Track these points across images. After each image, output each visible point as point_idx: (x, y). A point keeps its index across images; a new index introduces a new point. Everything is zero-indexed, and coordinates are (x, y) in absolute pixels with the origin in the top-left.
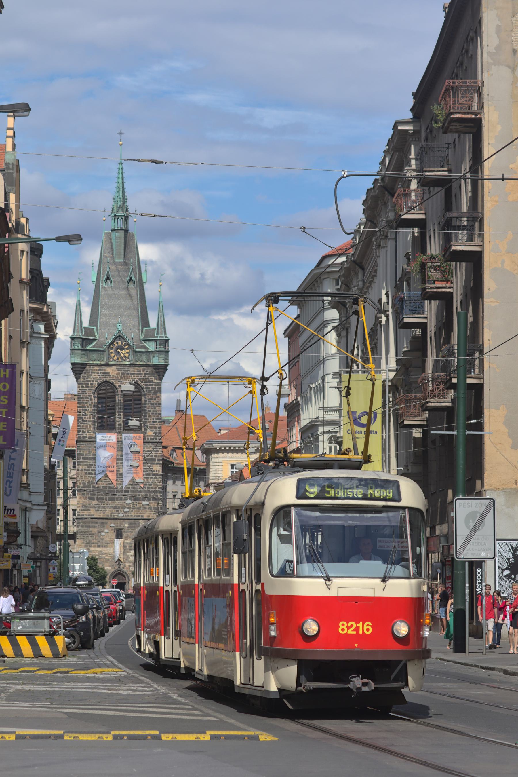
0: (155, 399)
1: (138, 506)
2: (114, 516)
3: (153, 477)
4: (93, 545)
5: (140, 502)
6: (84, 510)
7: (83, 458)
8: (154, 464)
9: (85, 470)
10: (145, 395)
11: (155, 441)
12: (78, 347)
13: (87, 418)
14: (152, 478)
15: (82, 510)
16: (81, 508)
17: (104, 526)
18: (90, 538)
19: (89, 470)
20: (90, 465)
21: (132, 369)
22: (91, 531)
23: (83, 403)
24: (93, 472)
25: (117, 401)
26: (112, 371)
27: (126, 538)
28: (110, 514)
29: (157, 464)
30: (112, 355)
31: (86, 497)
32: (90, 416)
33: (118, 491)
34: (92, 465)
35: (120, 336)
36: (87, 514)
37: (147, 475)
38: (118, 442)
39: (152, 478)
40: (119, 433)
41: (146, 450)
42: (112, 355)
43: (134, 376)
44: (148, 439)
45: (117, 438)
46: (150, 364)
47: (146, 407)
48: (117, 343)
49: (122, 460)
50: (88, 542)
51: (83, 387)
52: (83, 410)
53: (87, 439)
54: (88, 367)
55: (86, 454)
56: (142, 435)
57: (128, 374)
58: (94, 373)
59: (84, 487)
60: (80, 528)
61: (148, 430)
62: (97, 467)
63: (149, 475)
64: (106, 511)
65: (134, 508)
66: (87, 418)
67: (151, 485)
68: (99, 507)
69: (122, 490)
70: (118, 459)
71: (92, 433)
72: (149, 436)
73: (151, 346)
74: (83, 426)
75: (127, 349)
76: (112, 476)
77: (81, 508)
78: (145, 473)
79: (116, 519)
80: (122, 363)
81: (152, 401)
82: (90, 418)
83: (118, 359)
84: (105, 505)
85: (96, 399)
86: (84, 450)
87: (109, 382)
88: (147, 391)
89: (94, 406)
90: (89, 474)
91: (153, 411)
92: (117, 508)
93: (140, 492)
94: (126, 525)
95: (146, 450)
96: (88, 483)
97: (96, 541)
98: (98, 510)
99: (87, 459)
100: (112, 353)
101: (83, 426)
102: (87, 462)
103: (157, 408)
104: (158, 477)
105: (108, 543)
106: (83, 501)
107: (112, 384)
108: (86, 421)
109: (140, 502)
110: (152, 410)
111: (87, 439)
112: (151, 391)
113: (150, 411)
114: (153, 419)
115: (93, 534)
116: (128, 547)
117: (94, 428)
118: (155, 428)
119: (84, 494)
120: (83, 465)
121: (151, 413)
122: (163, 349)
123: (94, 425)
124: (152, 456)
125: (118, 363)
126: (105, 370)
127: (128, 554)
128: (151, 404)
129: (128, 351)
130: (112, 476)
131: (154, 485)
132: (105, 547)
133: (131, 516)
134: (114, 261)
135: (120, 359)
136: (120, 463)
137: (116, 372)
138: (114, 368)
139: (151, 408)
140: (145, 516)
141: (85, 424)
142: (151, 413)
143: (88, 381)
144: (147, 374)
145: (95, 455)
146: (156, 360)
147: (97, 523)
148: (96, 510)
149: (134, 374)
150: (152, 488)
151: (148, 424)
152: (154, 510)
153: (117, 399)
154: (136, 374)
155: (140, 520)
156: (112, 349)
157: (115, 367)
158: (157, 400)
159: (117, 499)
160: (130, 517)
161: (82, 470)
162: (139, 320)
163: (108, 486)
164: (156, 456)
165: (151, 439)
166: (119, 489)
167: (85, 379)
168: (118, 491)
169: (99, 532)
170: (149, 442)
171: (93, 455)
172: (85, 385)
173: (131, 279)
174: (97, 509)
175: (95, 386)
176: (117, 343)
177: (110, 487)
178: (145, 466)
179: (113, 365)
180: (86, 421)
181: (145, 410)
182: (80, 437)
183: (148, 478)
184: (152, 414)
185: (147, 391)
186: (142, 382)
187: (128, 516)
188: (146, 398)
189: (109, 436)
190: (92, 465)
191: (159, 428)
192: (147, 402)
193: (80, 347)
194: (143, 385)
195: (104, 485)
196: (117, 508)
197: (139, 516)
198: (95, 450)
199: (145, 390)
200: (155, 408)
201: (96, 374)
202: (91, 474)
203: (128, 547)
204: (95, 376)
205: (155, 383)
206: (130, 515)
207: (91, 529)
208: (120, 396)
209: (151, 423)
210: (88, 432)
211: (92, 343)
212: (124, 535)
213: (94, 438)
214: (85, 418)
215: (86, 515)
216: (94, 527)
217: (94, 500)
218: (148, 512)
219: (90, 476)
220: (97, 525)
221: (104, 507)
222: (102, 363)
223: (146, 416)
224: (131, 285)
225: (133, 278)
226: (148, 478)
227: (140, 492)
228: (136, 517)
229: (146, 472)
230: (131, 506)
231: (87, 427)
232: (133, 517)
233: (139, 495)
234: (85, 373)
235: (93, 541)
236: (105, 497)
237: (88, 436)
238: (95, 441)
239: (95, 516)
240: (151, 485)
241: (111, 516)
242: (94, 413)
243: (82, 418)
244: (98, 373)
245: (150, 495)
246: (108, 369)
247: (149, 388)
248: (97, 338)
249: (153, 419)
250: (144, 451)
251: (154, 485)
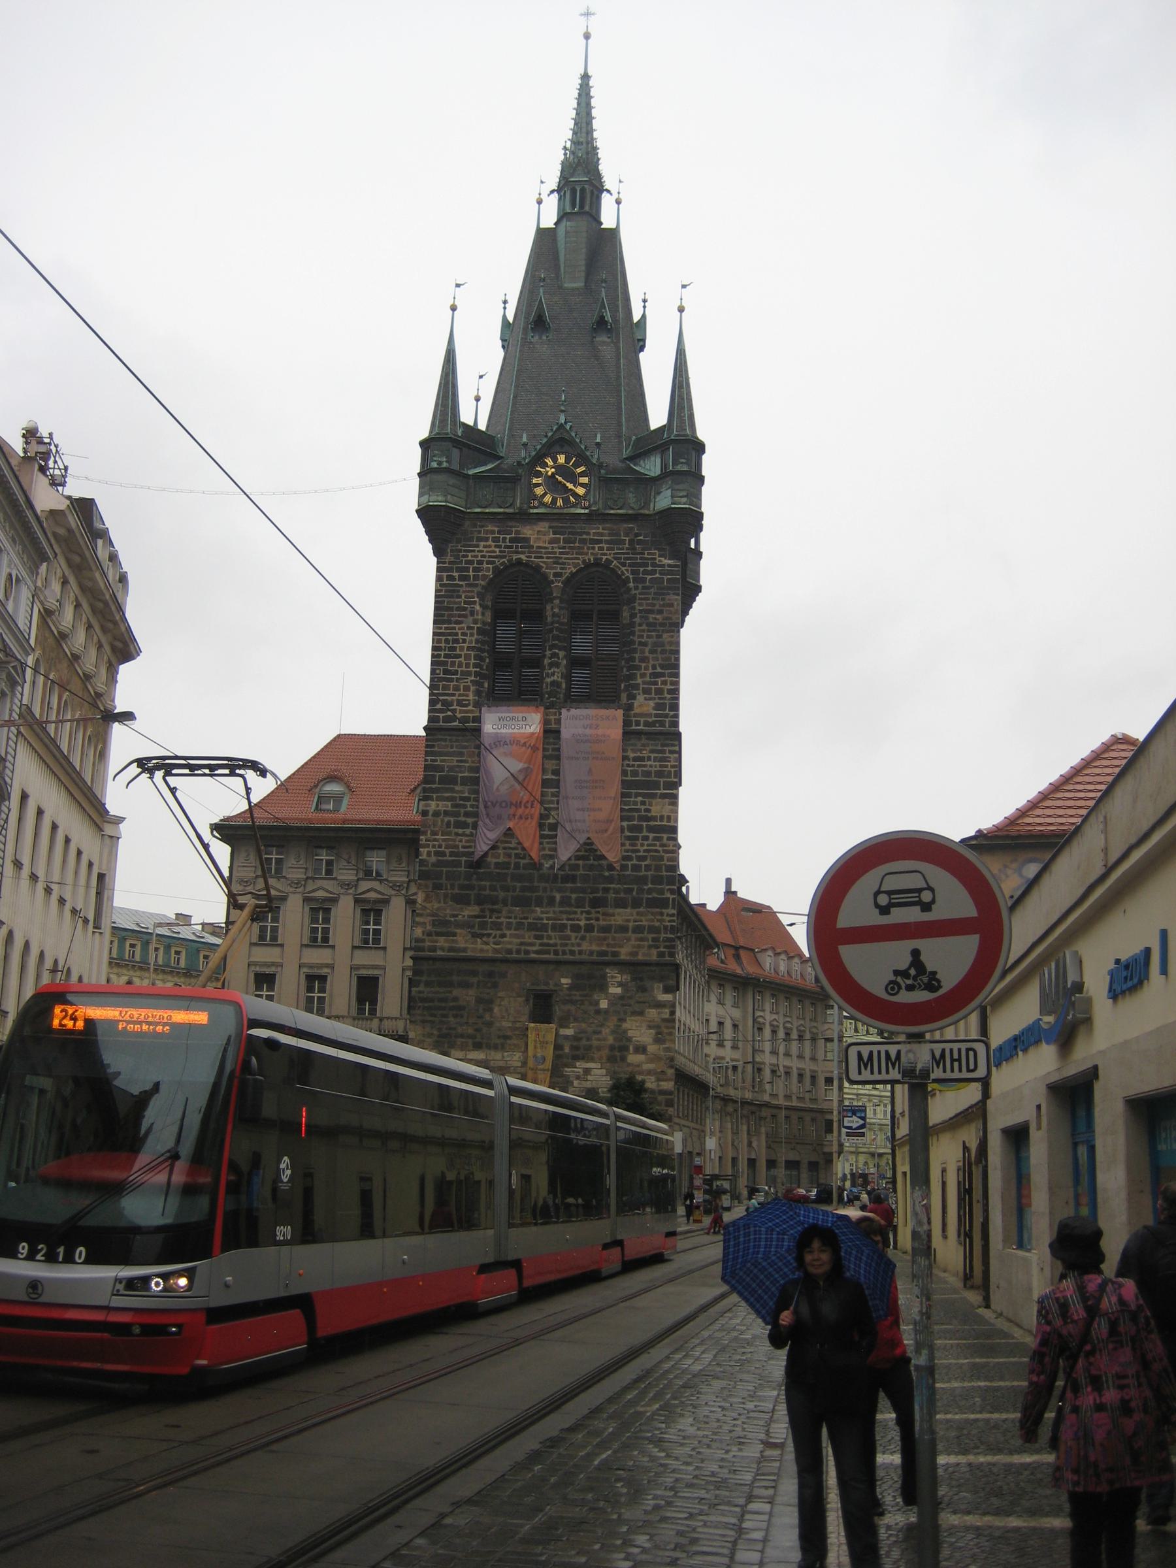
0: (660, 612)
1: (602, 923)
2: (527, 952)
3: (651, 835)
4: (459, 1041)
5: (611, 911)
6: (438, 934)
7: (443, 780)
8: (653, 796)
9: (446, 813)
10: (633, 599)
11: (658, 728)
12: (440, 463)
13: (460, 665)
14: (646, 838)
15: (429, 934)
16: (429, 928)
17: (495, 986)
18: (451, 1019)
19: (457, 814)
20: (462, 799)
21: (596, 530)
22: (456, 999)
23: (449, 622)
24: (470, 820)
25: (549, 619)
26: (537, 535)
27: (563, 1023)
28: (514, 948)
29: (664, 796)
30: (539, 491)
31: (446, 896)
32: (467, 657)
33: (543, 878)
34: (468, 799)
35: (562, 440)
36: (446, 945)
37: (632, 829)
38: (546, 731)
39: (646, 838)
40: (552, 705)
41: (632, 755)
42: (539, 491)
43: (600, 549)
44: (638, 724)
45: (546, 722)
46: (647, 512)
47: (633, 633)
48: (555, 460)
49: (556, 783)
50: (444, 1031)
51: (450, 578)
52: (447, 641)
53: (456, 723)
54: (467, 523)
55: (451, 768)
56: (620, 713)
57: (583, 541)
58: (487, 540)
59: (439, 864)
60: (422, 988)
61: (640, 698)
62: (481, 806)
63: (639, 829)
64: (503, 936)
65: (589, 929)
66: (460, 665)
67: (644, 858)
68: (483, 925)
69: (556, 876)
70: (545, 783)
71: (470, 708)
72: (641, 715)
73: (652, 466)
74: (445, 688)
75: (582, 474)
76: (528, 835)
77: (429, 928)
78: (625, 824)
79: (533, 961)
80: (565, 511)
81: (651, 616)
82: (468, 665)
83: (554, 501)
84: (502, 920)
85: (488, 614)
86: (446, 754)
87: (527, 565)
88: (636, 588)
89: (481, 631)
90: (458, 825)
91: (655, 644)
92: (537, 928)
93: (610, 880)
94: (564, 981)
95: (632, 755)
96: (452, 854)
97: (471, 1031)
98: (481, 936)
99: (452, 780)
100: (538, 485)
101: (445, 688)
102: (453, 791)
103: (665, 635)
104: (665, 836)
105: (506, 1037)
106: (436, 905)
107: (537, 569)
108: (456, 673)
109: (611, 911)
110: (650, 640)
111: (456, 723)
112: (649, 588)
113: (645, 644)
114: (654, 667)
115: (461, 1008)
116: (567, 1050)
117: (478, 693)
118: (659, 692)
119: (437, 887)
120: (438, 799)
121: (647, 649)
122: (685, 468)
123: (481, 685)
124: (648, 774)
125: (555, 511)
126: (517, 532)
127: (568, 1071)
128: (649, 625)
129: (585, 480)
130: (528, 835)
131: (654, 858)
132: (496, 1047)
133: (580, 953)
134: (560, 287)
135: (560, 502)
136: (553, 795)
137: (547, 538)
138: (543, 526)
139: (649, 637)
140: (624, 953)
141: (451, 680)
142: (647, 649)
143: (468, 562)
144: (639, 542)
145: (477, 770)
146: (663, 500)
147: (474, 973)
148: (475, 935)
149: (600, 542)
150: (648, 868)
151: (639, 681)
152: (650, 936)
153: (549, 613)
154: (607, 542)
155: (608, 964)
156: (539, 474)
157: (546, 524)
158: (665, 614)
159: (539, 903)
160: (577, 957)
161: (436, 814)
162: (620, 414)
163: (513, 860)
164: (660, 774)
165: (647, 724)
166: (545, 871)
167: (457, 557)
168: (543, 878)
169: (479, 1001)
170: (639, 734)
171: (471, 769)
172: (456, 574)
173: (601, 323)
174: (476, 930)
175: (485, 577)
176: (555, 460)
177: (517, 866)
178: (626, 804)
179: (540, 517)
180: (456, 673)
181: (633, 642)
182: (430, 719)
183: (636, 838)
184: (652, 652)
185: (636, 588)
186: (624, 565)
187: (572, 953)
188: (634, 608)
189: (520, 715)
190: (468, 799)
191: (670, 692)
192: (637, 620)
193: (445, 465)
194: (626, 572)
195: (501, 859)
196: (537, 928)
197: (604, 953)
198: (479, 755)
199: (631, 585)
200: (659, 637)
201: (490, 543)
202: (465, 825)
203: (567, 1050)
204: (487, 551)
205: (663, 566)
206: (576, 949)
207: (456, 992)
208: (557, 602)
209: (648, 679)
210: (460, 703)
211: (486, 464)
212: (558, 1010)
213: (478, 719)
214: (453, 664)
215: (442, 949)
216: (466, 985)
217: (468, 904)
218: (633, 942)
219: (460, 831)
220: (475, 980)
221: (497, 926)
222: (511, 510)
223: (633, 659)
224: (602, 338)
225: (608, 317)
226: (636, 838)
227: (610, 880)
228: (595, 958)
229: (629, 819)
230: (582, 923)
231: (457, 688)
232: (584, 957)
233: (606, 890)
234: (459, 541)
235: (460, 1030)
236: (502, 894)
237: (459, 715)
238: (477, 731)
239: (469, 954)
240: (644, 858)
241: (518, 952)
242: (479, 649)
243: (444, 663)
244: (495, 540)
245: (640, 891)
246: (528, 532)
247: (643, 580)
248: (502, 452)
249: (654, 667)
250: (625, 758)
251: (654, 858)
